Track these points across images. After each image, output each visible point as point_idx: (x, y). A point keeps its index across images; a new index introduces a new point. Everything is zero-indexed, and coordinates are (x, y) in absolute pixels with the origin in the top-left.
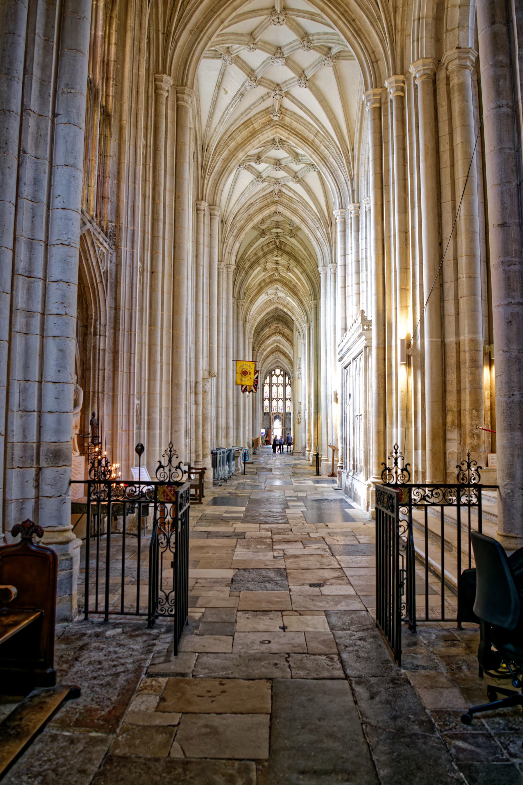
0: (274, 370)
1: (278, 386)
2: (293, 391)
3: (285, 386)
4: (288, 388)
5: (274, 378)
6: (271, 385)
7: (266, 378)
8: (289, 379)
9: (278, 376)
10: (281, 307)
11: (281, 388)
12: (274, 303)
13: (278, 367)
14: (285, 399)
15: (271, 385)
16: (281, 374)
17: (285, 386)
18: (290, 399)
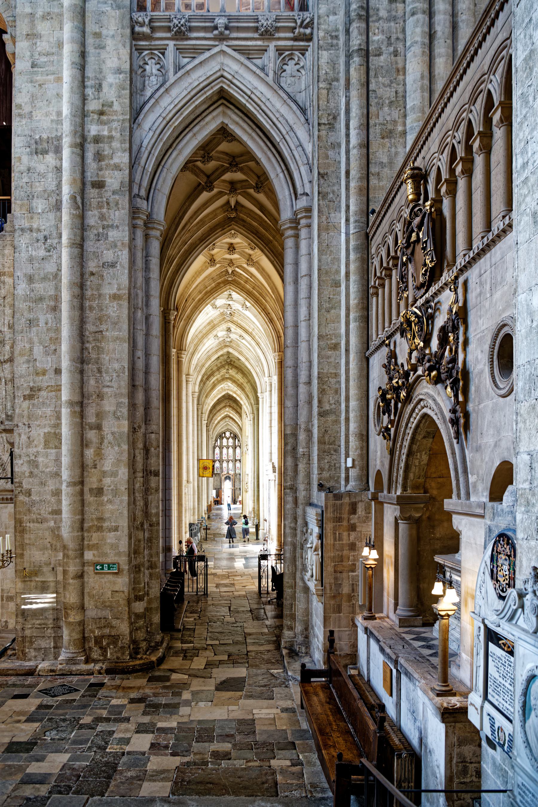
0: (225, 433)
2: (242, 453)
3: (235, 448)
4: (238, 450)
5: (225, 440)
6: (221, 448)
7: (216, 441)
9: (228, 439)
11: (231, 450)
16: (231, 436)
17: (235, 448)
18: (240, 461)
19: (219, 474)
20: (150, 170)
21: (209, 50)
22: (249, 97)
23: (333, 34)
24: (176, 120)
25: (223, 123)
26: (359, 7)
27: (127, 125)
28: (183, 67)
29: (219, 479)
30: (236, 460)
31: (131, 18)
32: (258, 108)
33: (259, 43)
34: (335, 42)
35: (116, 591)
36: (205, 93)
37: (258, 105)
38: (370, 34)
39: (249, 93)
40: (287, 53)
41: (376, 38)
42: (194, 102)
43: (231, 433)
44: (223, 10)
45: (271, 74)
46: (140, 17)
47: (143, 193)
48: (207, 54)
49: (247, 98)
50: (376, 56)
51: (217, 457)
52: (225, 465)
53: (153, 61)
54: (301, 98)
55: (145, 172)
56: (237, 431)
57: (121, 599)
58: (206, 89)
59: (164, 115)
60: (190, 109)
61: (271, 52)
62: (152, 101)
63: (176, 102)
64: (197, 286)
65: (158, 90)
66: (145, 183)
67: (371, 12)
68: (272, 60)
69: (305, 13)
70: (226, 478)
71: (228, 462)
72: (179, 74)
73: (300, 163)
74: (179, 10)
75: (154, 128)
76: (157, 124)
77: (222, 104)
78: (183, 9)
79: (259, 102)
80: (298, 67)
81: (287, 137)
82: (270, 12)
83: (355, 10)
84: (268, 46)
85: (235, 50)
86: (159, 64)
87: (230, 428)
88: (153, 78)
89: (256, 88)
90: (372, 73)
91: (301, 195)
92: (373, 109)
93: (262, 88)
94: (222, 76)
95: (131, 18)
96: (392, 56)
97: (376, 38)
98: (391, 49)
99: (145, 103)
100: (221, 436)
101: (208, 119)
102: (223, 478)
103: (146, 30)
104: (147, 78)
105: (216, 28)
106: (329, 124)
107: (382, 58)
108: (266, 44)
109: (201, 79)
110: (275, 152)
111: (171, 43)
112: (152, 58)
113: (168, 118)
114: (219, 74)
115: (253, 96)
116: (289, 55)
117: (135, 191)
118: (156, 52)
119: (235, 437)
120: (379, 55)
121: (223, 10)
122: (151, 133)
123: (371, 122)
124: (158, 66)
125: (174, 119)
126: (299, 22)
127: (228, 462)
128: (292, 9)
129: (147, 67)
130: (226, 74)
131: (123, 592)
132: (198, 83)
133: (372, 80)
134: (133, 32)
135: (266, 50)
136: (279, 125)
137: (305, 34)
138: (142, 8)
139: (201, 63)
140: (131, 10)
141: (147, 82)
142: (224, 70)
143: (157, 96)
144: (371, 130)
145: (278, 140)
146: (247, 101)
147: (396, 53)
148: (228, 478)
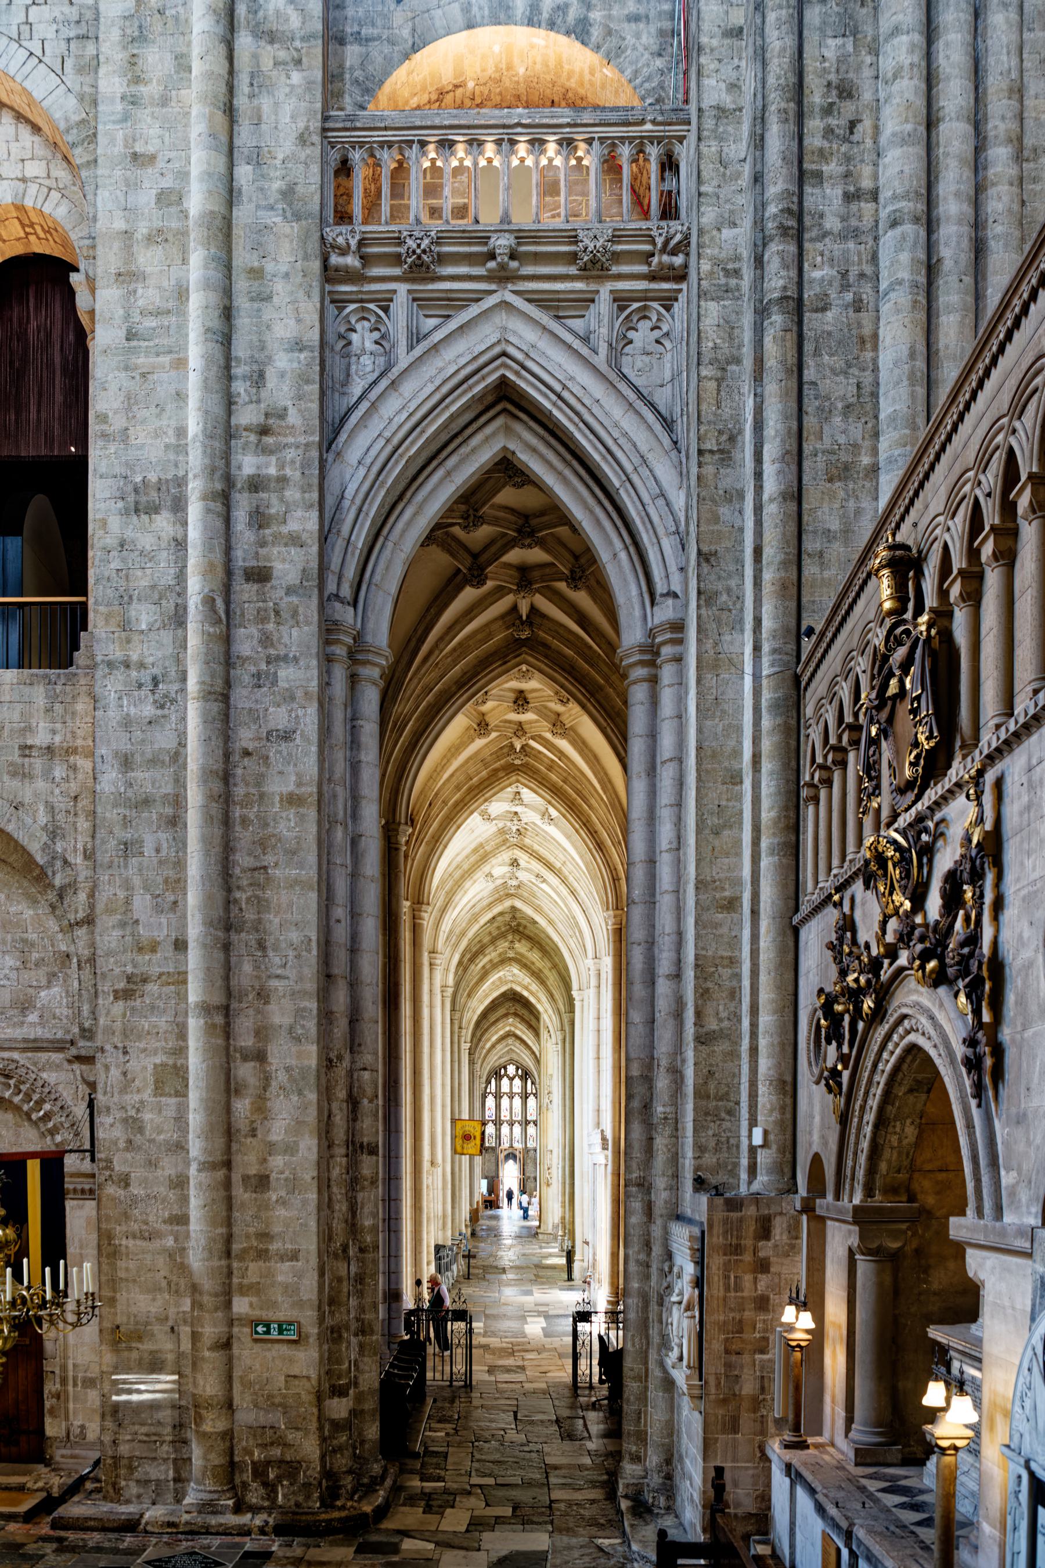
0: (505, 1068)
1: (511, 1098)
2: (540, 1108)
3: (525, 1097)
4: (532, 1101)
5: (505, 1082)
6: (498, 1096)
7: (488, 1082)
9: (511, 1079)
11: (517, 1102)
13: (511, 1061)
15: (498, 1096)
17: (525, 1097)
18: (535, 1123)
19: (493, 1149)
20: (360, 545)
21: (478, 300)
22: (559, 397)
23: (730, 266)
24: (413, 443)
25: (505, 448)
26: (782, 211)
27: (315, 454)
28: (426, 336)
30: (527, 1122)
31: (322, 238)
32: (576, 419)
33: (579, 285)
34: (733, 282)
35: (295, 1377)
36: (470, 388)
37: (577, 413)
38: (806, 265)
39: (558, 388)
40: (636, 305)
41: (818, 274)
42: (447, 407)
43: (517, 1069)
44: (506, 219)
45: (603, 349)
46: (338, 234)
47: (346, 591)
48: (474, 310)
49: (554, 398)
50: (816, 311)
51: (490, 1113)
52: (505, 1129)
53: (366, 324)
54: (662, 398)
55: (350, 549)
56: (530, 1063)
57: (304, 1391)
58: (471, 381)
59: (387, 434)
60: (440, 421)
61: (604, 304)
62: (365, 406)
63: (412, 406)
64: (452, 775)
65: (375, 383)
66: (351, 572)
67: (808, 221)
68: (606, 320)
69: (672, 223)
70: (508, 1157)
71: (511, 1124)
72: (418, 351)
73: (661, 531)
74: (418, 222)
75: (368, 460)
76: (373, 453)
77: (505, 410)
78: (425, 218)
79: (579, 407)
80: (657, 333)
81: (635, 478)
82: (600, 222)
83: (775, 215)
84: (598, 292)
85: (529, 301)
86: (378, 330)
87: (515, 1057)
88: (366, 360)
89: (572, 378)
90: (808, 347)
91: (663, 595)
92: (810, 421)
93: (584, 377)
94: (504, 354)
95: (322, 238)
96: (851, 310)
97: (817, 274)
98: (849, 297)
99: (350, 411)
100: (497, 1074)
101: (475, 441)
102: (502, 1156)
103: (351, 261)
104: (354, 359)
105: (492, 256)
106: (721, 451)
107: (829, 315)
108: (593, 287)
109: (463, 361)
110: (610, 508)
111: (402, 288)
112: (364, 318)
113: (395, 441)
114: (497, 350)
115: (566, 394)
116: (639, 309)
117: (331, 587)
118: (371, 306)
119: (525, 1075)
120: (824, 309)
121: (506, 219)
122: (362, 471)
123: (807, 448)
124: (376, 335)
125: (407, 442)
126: (660, 241)
127: (511, 1124)
128: (646, 214)
129: (355, 337)
130: (511, 350)
131: (308, 1378)
132: (456, 368)
133: (809, 361)
134: (326, 266)
135: (593, 301)
136: (619, 454)
137: (671, 267)
138: (343, 217)
139: (461, 327)
140: (323, 222)
141: (353, 368)
142: (507, 341)
143: (373, 395)
144: (806, 464)
145: (617, 484)
146: (554, 404)
147: (858, 306)
148: (511, 1156)
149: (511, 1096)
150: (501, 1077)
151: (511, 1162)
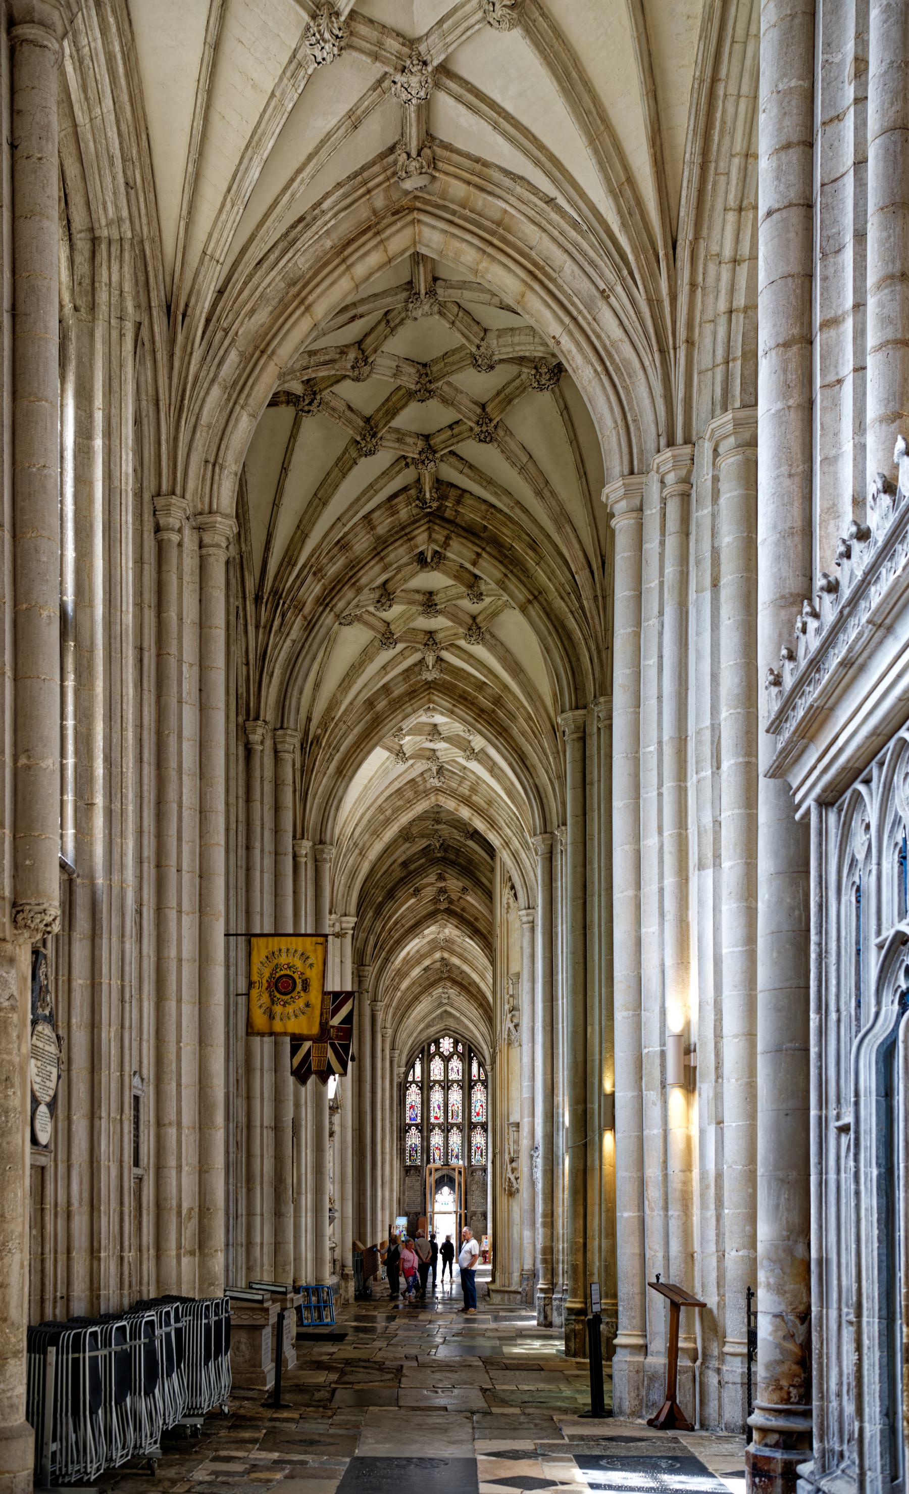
0: (437, 1043)
2: (493, 1101)
3: (468, 1086)
4: (479, 1095)
5: (437, 1066)
6: (426, 1086)
8: (480, 1065)
9: (446, 1060)
10: (450, 804)
11: (456, 1096)
12: (427, 793)
14: (468, 1127)
15: (426, 1086)
17: (468, 1086)
18: (484, 1127)
19: (417, 1169)
29: (418, 1185)
30: (472, 1126)
43: (456, 1043)
51: (413, 1114)
52: (437, 1139)
56: (477, 1030)
70: (440, 1184)
71: (446, 1129)
87: (452, 1023)
102: (431, 1180)
119: (469, 1053)
127: (446, 1129)
148: (445, 1180)
149: (446, 1086)
150: (430, 1058)
151: (446, 1190)
